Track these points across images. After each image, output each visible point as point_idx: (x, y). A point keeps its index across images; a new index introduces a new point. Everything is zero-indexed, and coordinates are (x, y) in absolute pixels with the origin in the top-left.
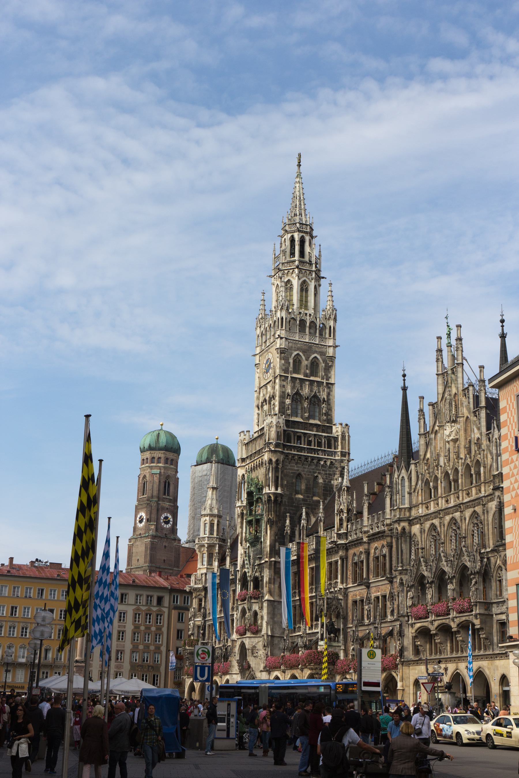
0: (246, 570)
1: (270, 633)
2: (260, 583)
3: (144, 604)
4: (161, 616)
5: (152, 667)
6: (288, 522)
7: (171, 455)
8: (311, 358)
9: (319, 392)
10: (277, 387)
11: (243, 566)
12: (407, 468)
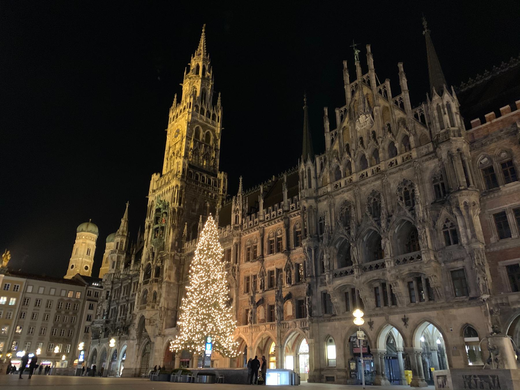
0: (150, 262)
1: (166, 306)
5: (66, 339)
6: (186, 228)
8: (206, 131)
9: (210, 152)
10: (184, 143)
11: (148, 259)
12: (313, 160)
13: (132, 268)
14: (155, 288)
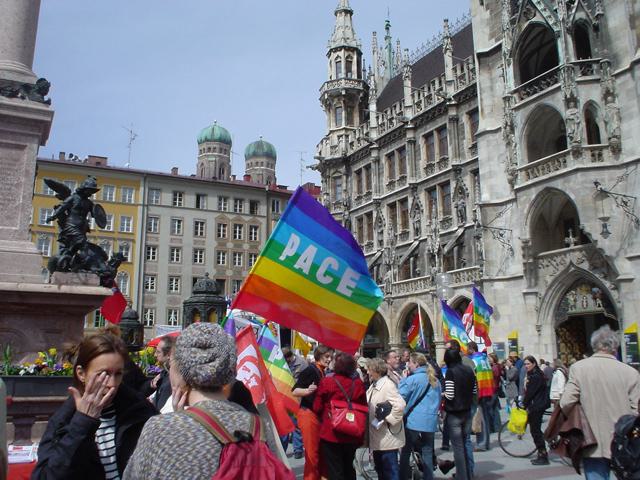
2: (591, 34)
3: (232, 210)
4: (256, 230)
7: (224, 146)
13: (408, 101)
14: (592, 93)
